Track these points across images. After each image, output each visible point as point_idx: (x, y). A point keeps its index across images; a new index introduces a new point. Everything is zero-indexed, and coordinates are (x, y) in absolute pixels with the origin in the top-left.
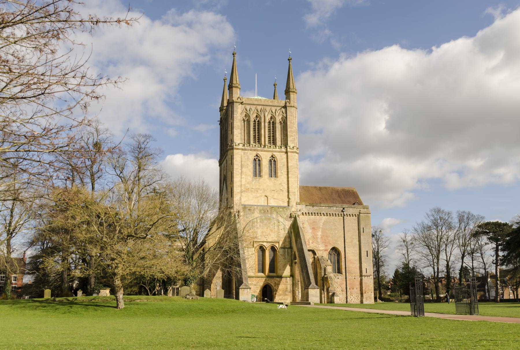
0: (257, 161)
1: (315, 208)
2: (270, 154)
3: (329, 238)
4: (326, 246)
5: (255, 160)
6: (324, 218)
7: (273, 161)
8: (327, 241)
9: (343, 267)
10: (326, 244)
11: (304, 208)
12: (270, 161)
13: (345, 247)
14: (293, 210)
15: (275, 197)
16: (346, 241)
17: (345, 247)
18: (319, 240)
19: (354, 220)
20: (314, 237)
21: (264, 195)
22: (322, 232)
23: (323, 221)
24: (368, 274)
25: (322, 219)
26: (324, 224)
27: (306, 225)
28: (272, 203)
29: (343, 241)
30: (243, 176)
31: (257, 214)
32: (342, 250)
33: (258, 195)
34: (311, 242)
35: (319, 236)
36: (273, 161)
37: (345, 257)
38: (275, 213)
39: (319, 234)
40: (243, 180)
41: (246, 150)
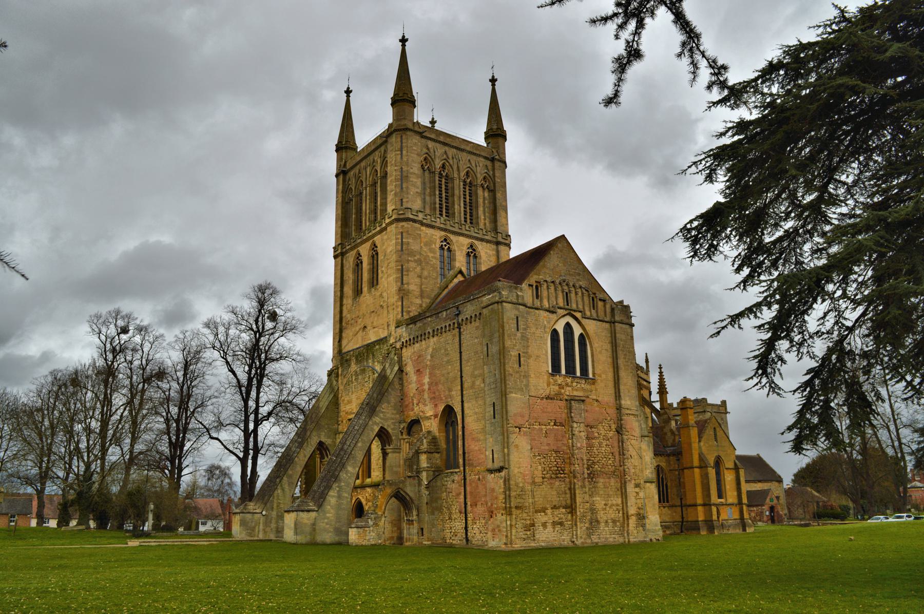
0: (358, 264)
1: (419, 324)
2: (368, 245)
3: (440, 386)
4: (436, 405)
5: (357, 265)
6: (433, 341)
7: (374, 255)
8: (437, 394)
9: (461, 452)
10: (434, 399)
11: (404, 333)
12: (373, 257)
13: (462, 402)
14: (392, 341)
15: (375, 324)
16: (466, 385)
17: (462, 402)
18: (426, 396)
19: (477, 328)
20: (420, 391)
21: (362, 326)
22: (431, 375)
23: (431, 350)
24: (497, 465)
25: (428, 347)
26: (432, 357)
27: (410, 369)
28: (373, 338)
29: (459, 388)
30: (345, 301)
31: (354, 367)
32: (457, 409)
33: (357, 329)
34: (415, 402)
35: (426, 387)
36: (374, 255)
37: (463, 427)
38: (371, 356)
39: (426, 380)
40: (344, 308)
41: (346, 252)
